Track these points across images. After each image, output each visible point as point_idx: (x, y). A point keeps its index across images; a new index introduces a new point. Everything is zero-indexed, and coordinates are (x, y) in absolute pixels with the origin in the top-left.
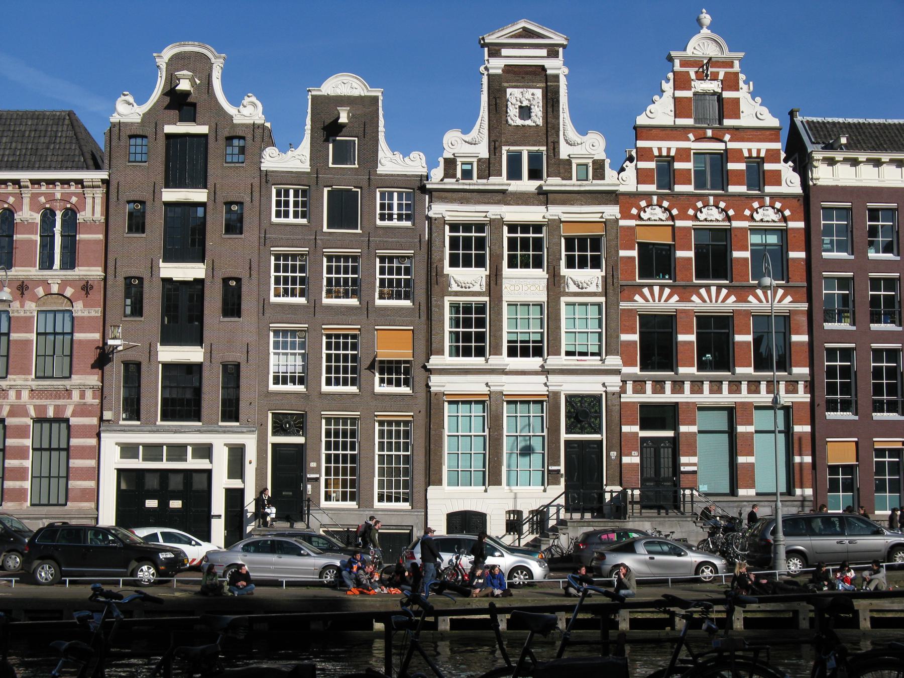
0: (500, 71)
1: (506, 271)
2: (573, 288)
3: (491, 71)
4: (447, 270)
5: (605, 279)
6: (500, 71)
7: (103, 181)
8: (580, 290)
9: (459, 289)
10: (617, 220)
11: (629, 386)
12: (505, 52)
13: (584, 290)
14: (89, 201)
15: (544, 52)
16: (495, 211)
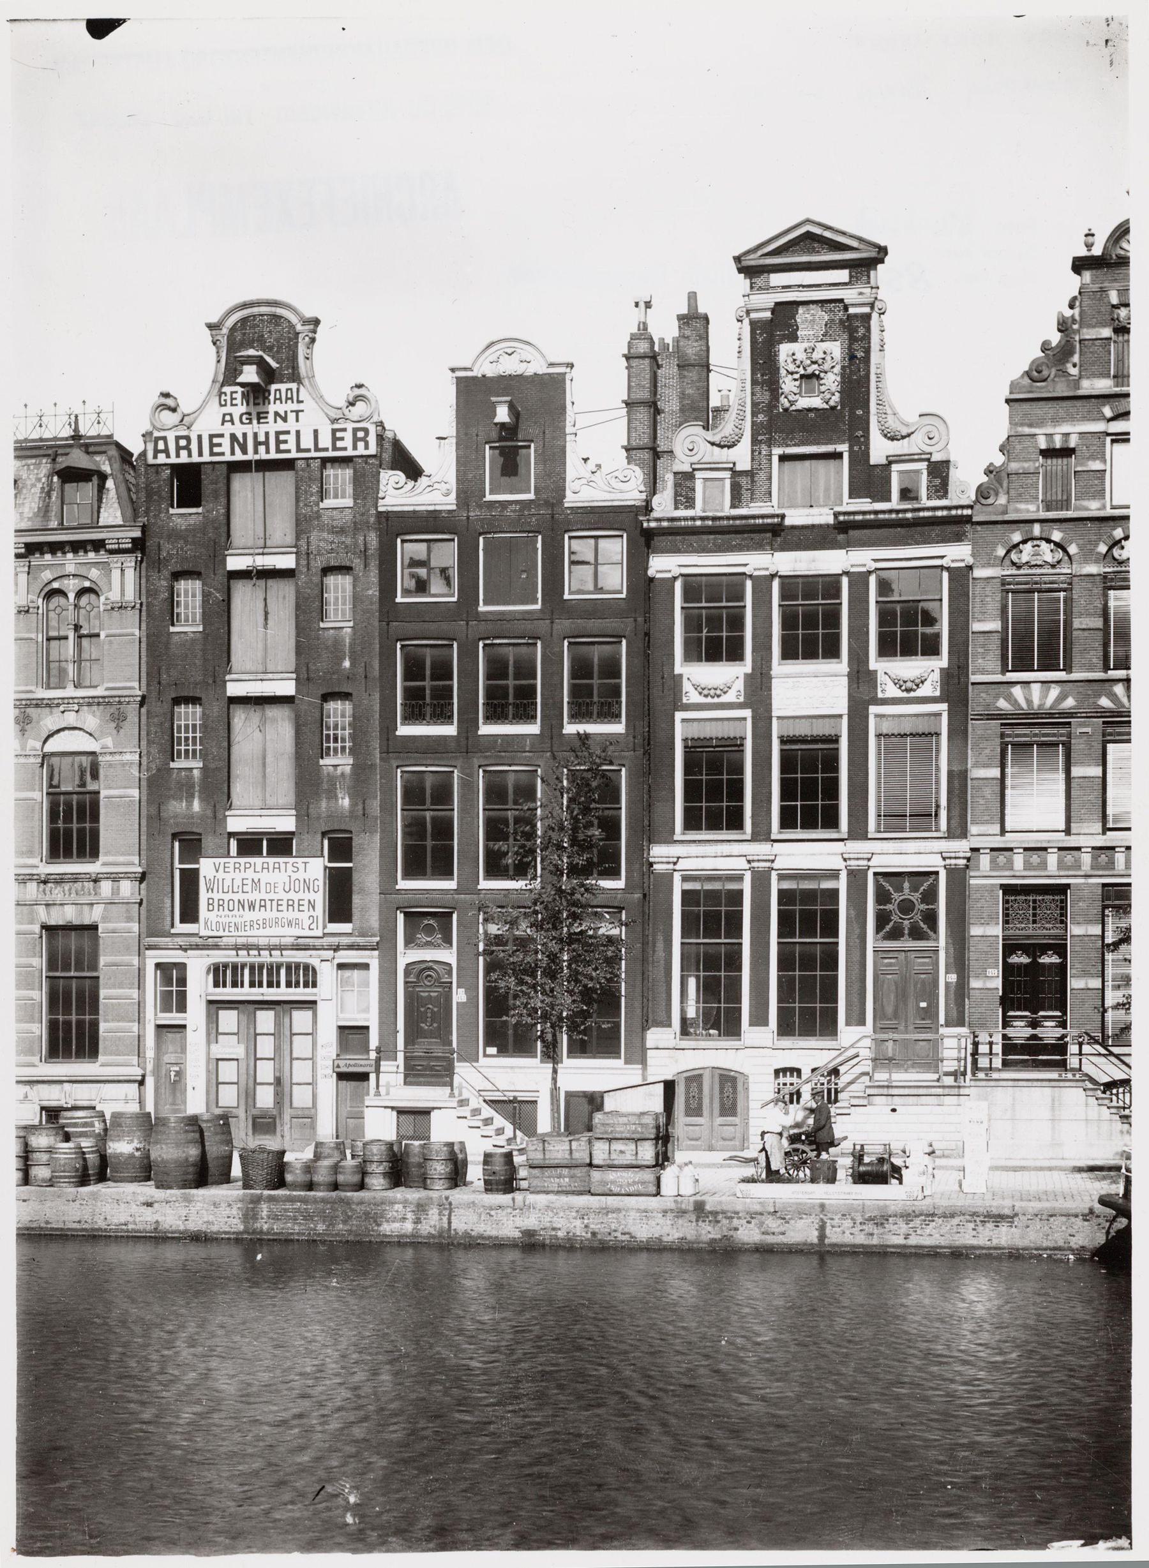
0: (768, 314)
1: (779, 668)
2: (893, 692)
3: (753, 315)
4: (680, 667)
5: (946, 675)
6: (768, 315)
7: (134, 540)
8: (905, 695)
9: (702, 700)
10: (970, 568)
11: (985, 860)
12: (777, 279)
13: (912, 694)
14: (116, 574)
15: (843, 275)
16: (758, 562)
